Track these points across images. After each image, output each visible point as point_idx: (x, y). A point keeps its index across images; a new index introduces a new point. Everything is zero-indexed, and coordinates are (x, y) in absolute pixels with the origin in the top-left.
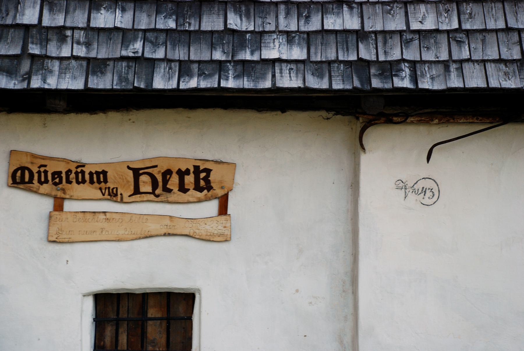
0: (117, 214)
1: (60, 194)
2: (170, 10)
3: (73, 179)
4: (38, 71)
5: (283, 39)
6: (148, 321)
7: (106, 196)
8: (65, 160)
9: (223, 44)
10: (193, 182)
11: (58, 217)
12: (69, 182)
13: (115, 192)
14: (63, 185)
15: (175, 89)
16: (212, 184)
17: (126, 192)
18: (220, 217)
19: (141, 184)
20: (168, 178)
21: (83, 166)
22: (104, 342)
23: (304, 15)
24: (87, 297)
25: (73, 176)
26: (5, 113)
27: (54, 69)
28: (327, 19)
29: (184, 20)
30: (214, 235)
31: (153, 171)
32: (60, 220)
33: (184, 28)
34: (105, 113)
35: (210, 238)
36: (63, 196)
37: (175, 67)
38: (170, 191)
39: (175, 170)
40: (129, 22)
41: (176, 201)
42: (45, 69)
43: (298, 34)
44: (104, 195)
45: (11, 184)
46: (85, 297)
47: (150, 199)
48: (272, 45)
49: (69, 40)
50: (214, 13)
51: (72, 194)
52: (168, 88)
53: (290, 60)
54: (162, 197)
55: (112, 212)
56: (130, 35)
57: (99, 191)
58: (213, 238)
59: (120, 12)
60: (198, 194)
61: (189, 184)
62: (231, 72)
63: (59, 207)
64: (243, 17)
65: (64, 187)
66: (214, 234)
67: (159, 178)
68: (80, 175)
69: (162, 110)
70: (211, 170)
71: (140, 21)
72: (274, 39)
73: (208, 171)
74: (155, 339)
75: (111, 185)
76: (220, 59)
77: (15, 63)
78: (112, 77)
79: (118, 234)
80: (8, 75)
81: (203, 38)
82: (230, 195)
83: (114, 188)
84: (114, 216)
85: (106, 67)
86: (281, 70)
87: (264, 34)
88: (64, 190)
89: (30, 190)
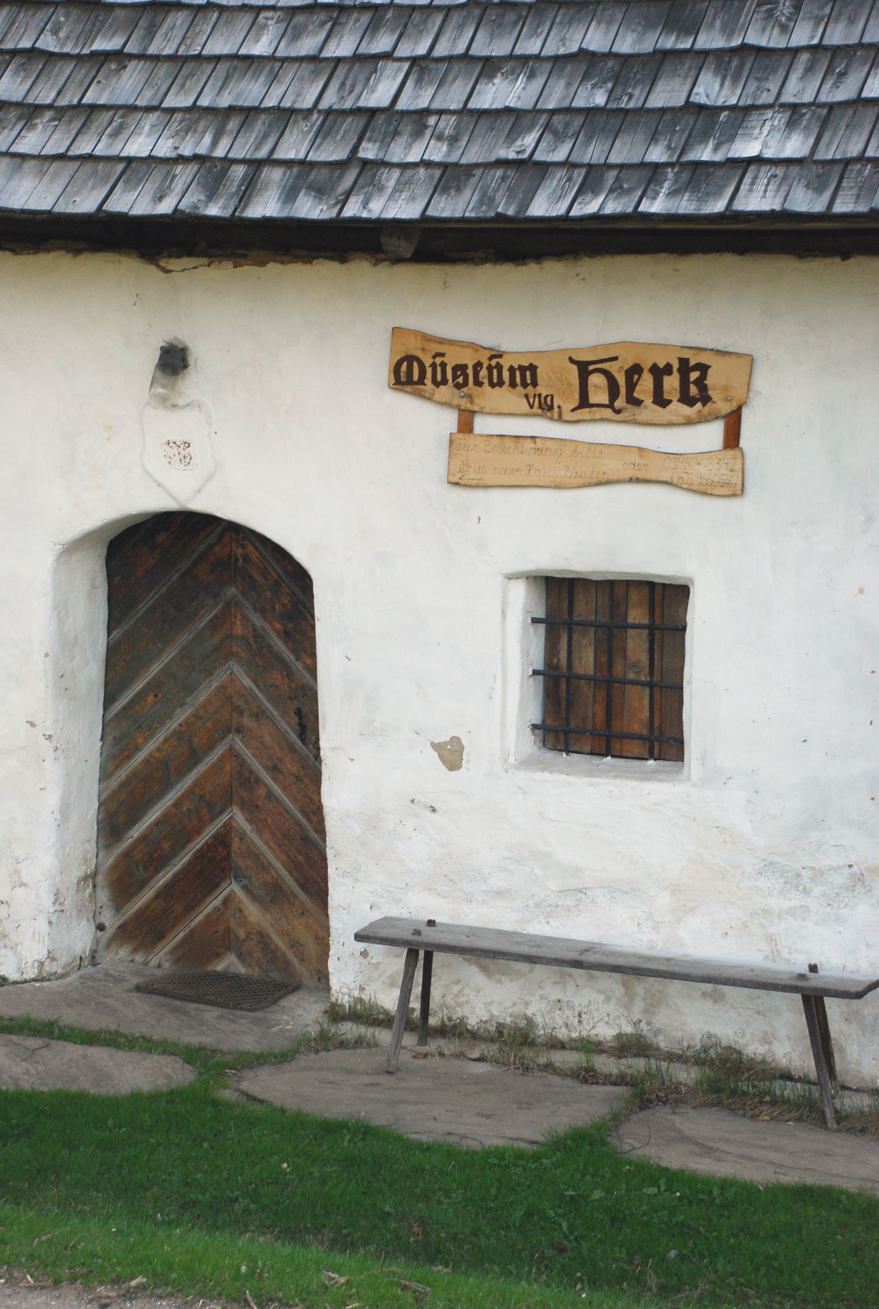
0: (554, 442)
1: (464, 403)
2: (608, 72)
3: (484, 378)
4: (362, 188)
5: (780, 119)
6: (628, 630)
7: (536, 410)
8: (472, 346)
9: (673, 132)
10: (678, 388)
11: (463, 442)
12: (478, 383)
13: (549, 402)
14: (470, 389)
15: (562, 216)
16: (710, 392)
17: (567, 402)
18: (723, 453)
19: (591, 389)
20: (635, 380)
21: (500, 356)
22: (558, 659)
23: (837, 71)
24: (515, 580)
25: (483, 373)
26: (387, 263)
27: (387, 185)
28: (875, 78)
29: (624, 90)
30: (712, 484)
31: (611, 367)
32: (466, 449)
33: (618, 104)
34: (539, 263)
35: (706, 489)
36: (469, 406)
37: (579, 176)
38: (638, 403)
39: (647, 365)
40: (532, 97)
41: (649, 422)
42: (374, 185)
43: (813, 108)
44: (531, 407)
45: (394, 384)
46: (512, 580)
47: (605, 416)
48: (757, 131)
49: (428, 133)
50: (679, 75)
51: (483, 404)
52: (551, 215)
53: (776, 159)
54: (625, 414)
55: (545, 438)
56: (526, 121)
57: (525, 400)
58: (712, 489)
59: (525, 79)
60: (686, 410)
61: (670, 392)
62: (666, 185)
63: (466, 426)
64: (728, 79)
65: (470, 392)
66: (712, 482)
67: (621, 381)
68: (495, 371)
69: (632, 257)
70: (709, 367)
71: (551, 95)
72: (765, 121)
73: (703, 368)
74: (639, 661)
75: (543, 390)
76: (657, 161)
77: (336, 175)
78: (470, 197)
79: (554, 475)
80: (318, 195)
81: (645, 123)
82: (746, 413)
83: (547, 396)
84: (549, 444)
85: (468, 179)
86: (755, 178)
87: (752, 110)
88: (470, 397)
89: (421, 395)
